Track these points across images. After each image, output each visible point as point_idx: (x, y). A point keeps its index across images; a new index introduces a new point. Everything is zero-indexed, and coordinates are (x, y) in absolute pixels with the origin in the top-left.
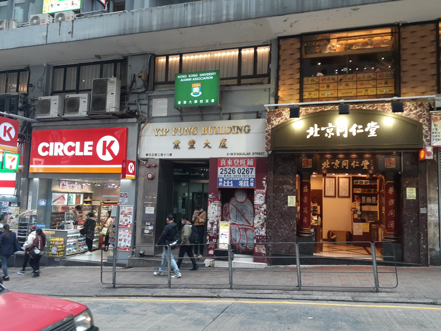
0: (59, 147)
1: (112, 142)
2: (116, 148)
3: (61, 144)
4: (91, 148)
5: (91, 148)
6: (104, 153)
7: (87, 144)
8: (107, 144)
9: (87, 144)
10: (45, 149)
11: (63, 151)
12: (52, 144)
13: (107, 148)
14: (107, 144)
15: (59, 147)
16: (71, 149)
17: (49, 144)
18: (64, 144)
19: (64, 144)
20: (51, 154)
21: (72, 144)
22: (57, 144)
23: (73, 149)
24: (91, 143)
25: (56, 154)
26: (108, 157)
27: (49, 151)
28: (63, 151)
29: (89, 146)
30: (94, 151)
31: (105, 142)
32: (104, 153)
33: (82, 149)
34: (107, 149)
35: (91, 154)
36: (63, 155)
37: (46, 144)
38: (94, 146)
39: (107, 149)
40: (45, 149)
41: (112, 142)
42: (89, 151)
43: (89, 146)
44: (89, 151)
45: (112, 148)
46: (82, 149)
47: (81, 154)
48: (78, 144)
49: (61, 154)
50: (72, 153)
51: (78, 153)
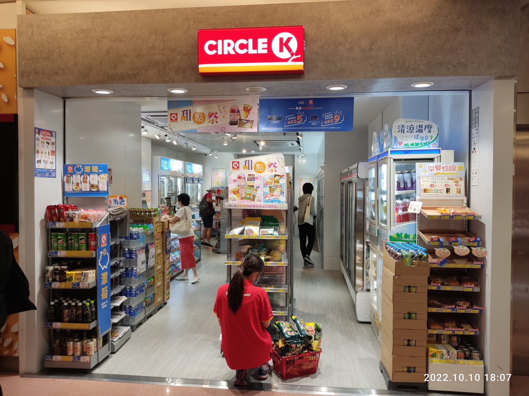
0: (229, 45)
1: (289, 39)
2: (294, 44)
6: (281, 50)
8: (284, 41)
10: (211, 47)
11: (234, 49)
12: (220, 42)
13: (284, 44)
14: (284, 41)
15: (229, 45)
16: (242, 47)
17: (217, 42)
18: (235, 42)
19: (235, 42)
20: (220, 53)
21: (244, 41)
22: (226, 42)
24: (266, 40)
25: (226, 53)
27: (217, 50)
28: (234, 49)
29: (263, 43)
30: (269, 48)
31: (281, 39)
32: (281, 50)
33: (255, 47)
34: (284, 46)
35: (266, 51)
36: (234, 53)
37: (213, 43)
38: (269, 43)
39: (284, 46)
40: (211, 47)
41: (289, 39)
42: (263, 49)
43: (263, 43)
44: (263, 49)
45: (290, 44)
46: (255, 47)
47: (255, 52)
48: (251, 41)
49: (232, 52)
50: (244, 51)
51: (251, 51)
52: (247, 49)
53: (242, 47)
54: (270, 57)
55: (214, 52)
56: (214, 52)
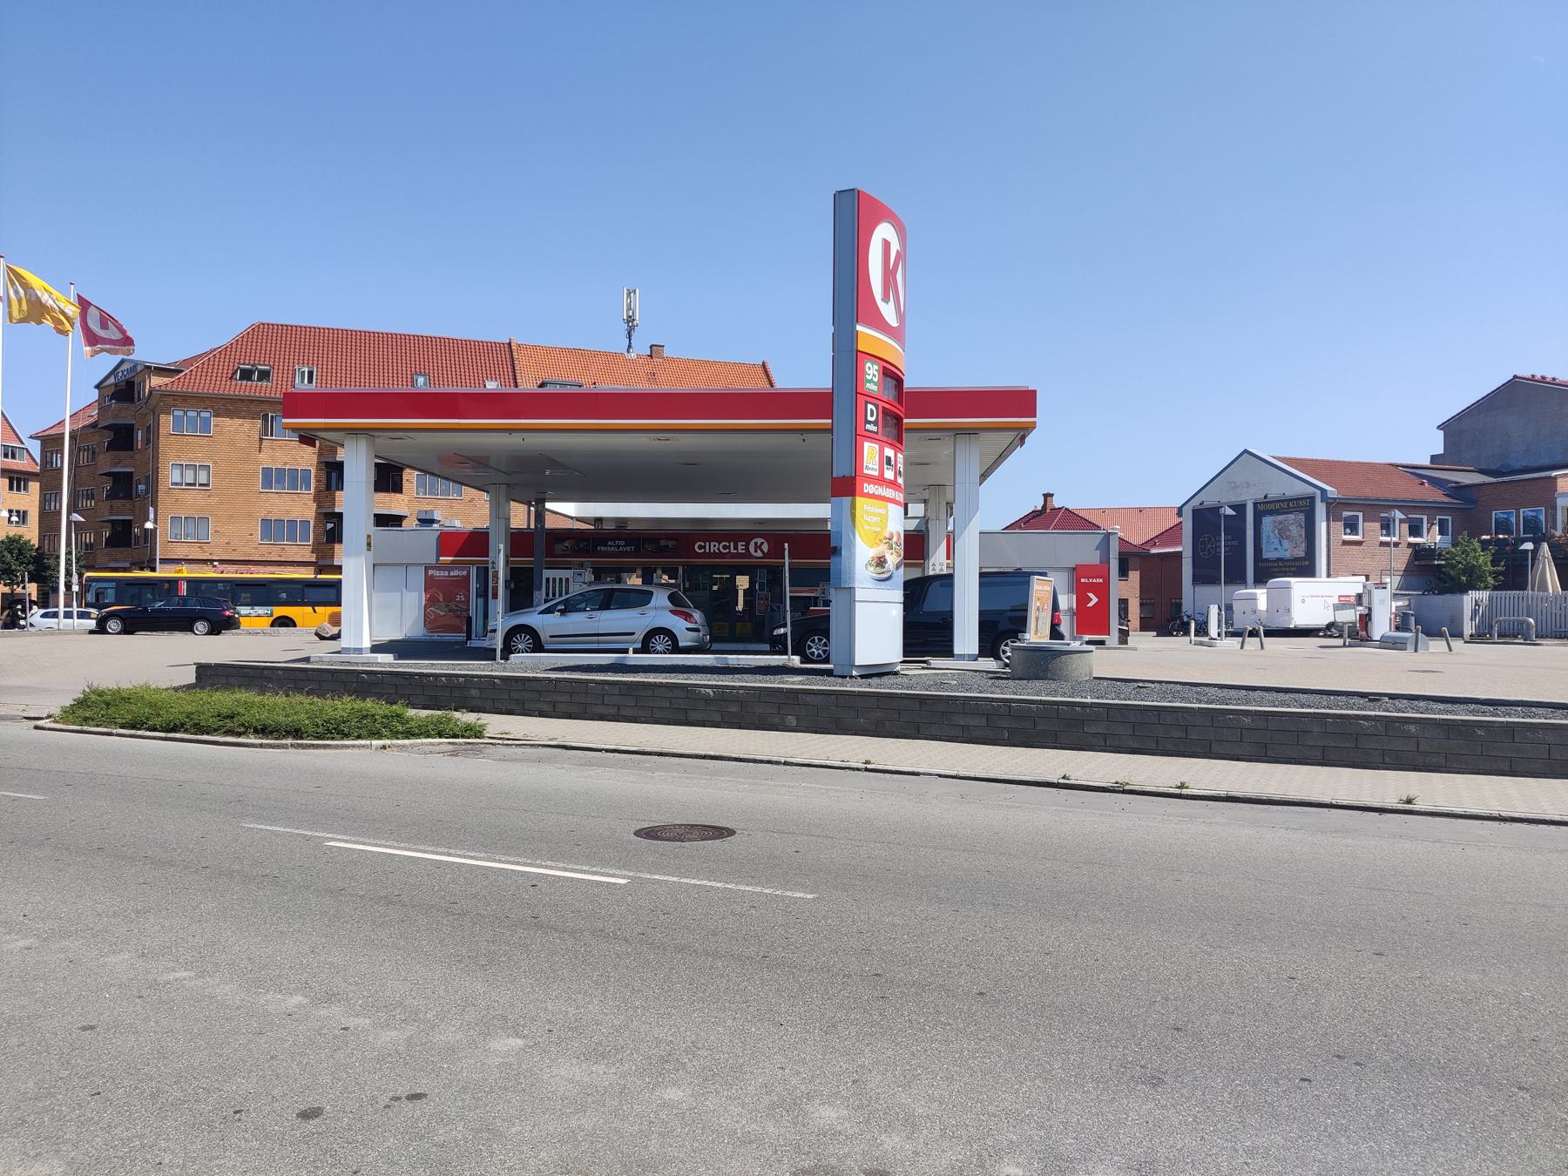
0: (715, 546)
1: (762, 543)
3: (717, 544)
6: (756, 551)
7: (740, 544)
9: (740, 544)
11: (718, 549)
13: (758, 547)
22: (712, 544)
23: (729, 547)
24: (744, 543)
25: (712, 551)
26: (759, 554)
28: (718, 549)
31: (756, 543)
32: (756, 551)
33: (736, 548)
41: (762, 543)
46: (736, 548)
47: (735, 551)
48: (732, 544)
49: (717, 551)
54: (748, 554)
55: (703, 550)
56: (703, 550)
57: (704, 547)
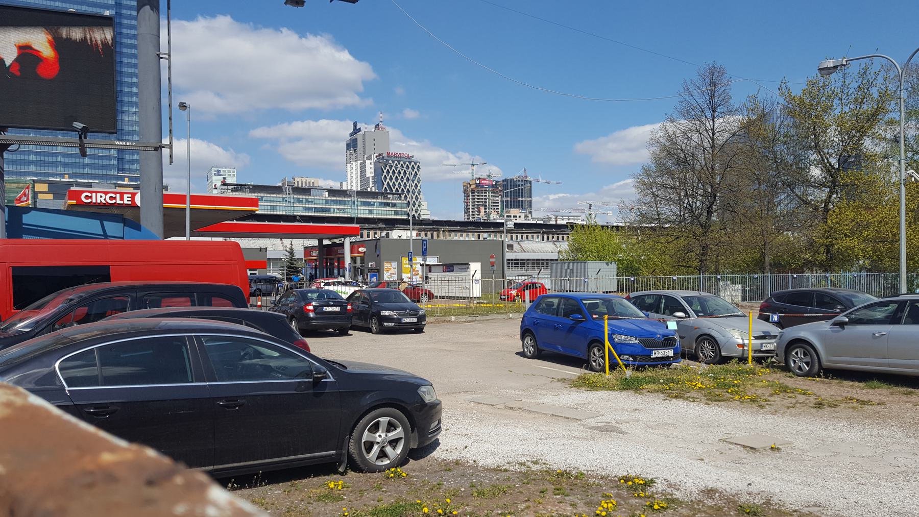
0: (101, 197)
4: (130, 199)
5: (130, 199)
10: (87, 197)
11: (105, 199)
18: (106, 195)
19: (106, 195)
20: (94, 201)
23: (115, 198)
25: (99, 201)
27: (92, 199)
28: (105, 199)
29: (128, 197)
33: (122, 199)
35: (130, 203)
40: (87, 197)
42: (128, 201)
43: (128, 197)
44: (128, 201)
46: (122, 199)
47: (122, 202)
49: (104, 202)
50: (114, 201)
51: (119, 202)
52: (116, 200)
53: (111, 198)
55: (89, 200)
56: (89, 200)
57: (91, 197)
